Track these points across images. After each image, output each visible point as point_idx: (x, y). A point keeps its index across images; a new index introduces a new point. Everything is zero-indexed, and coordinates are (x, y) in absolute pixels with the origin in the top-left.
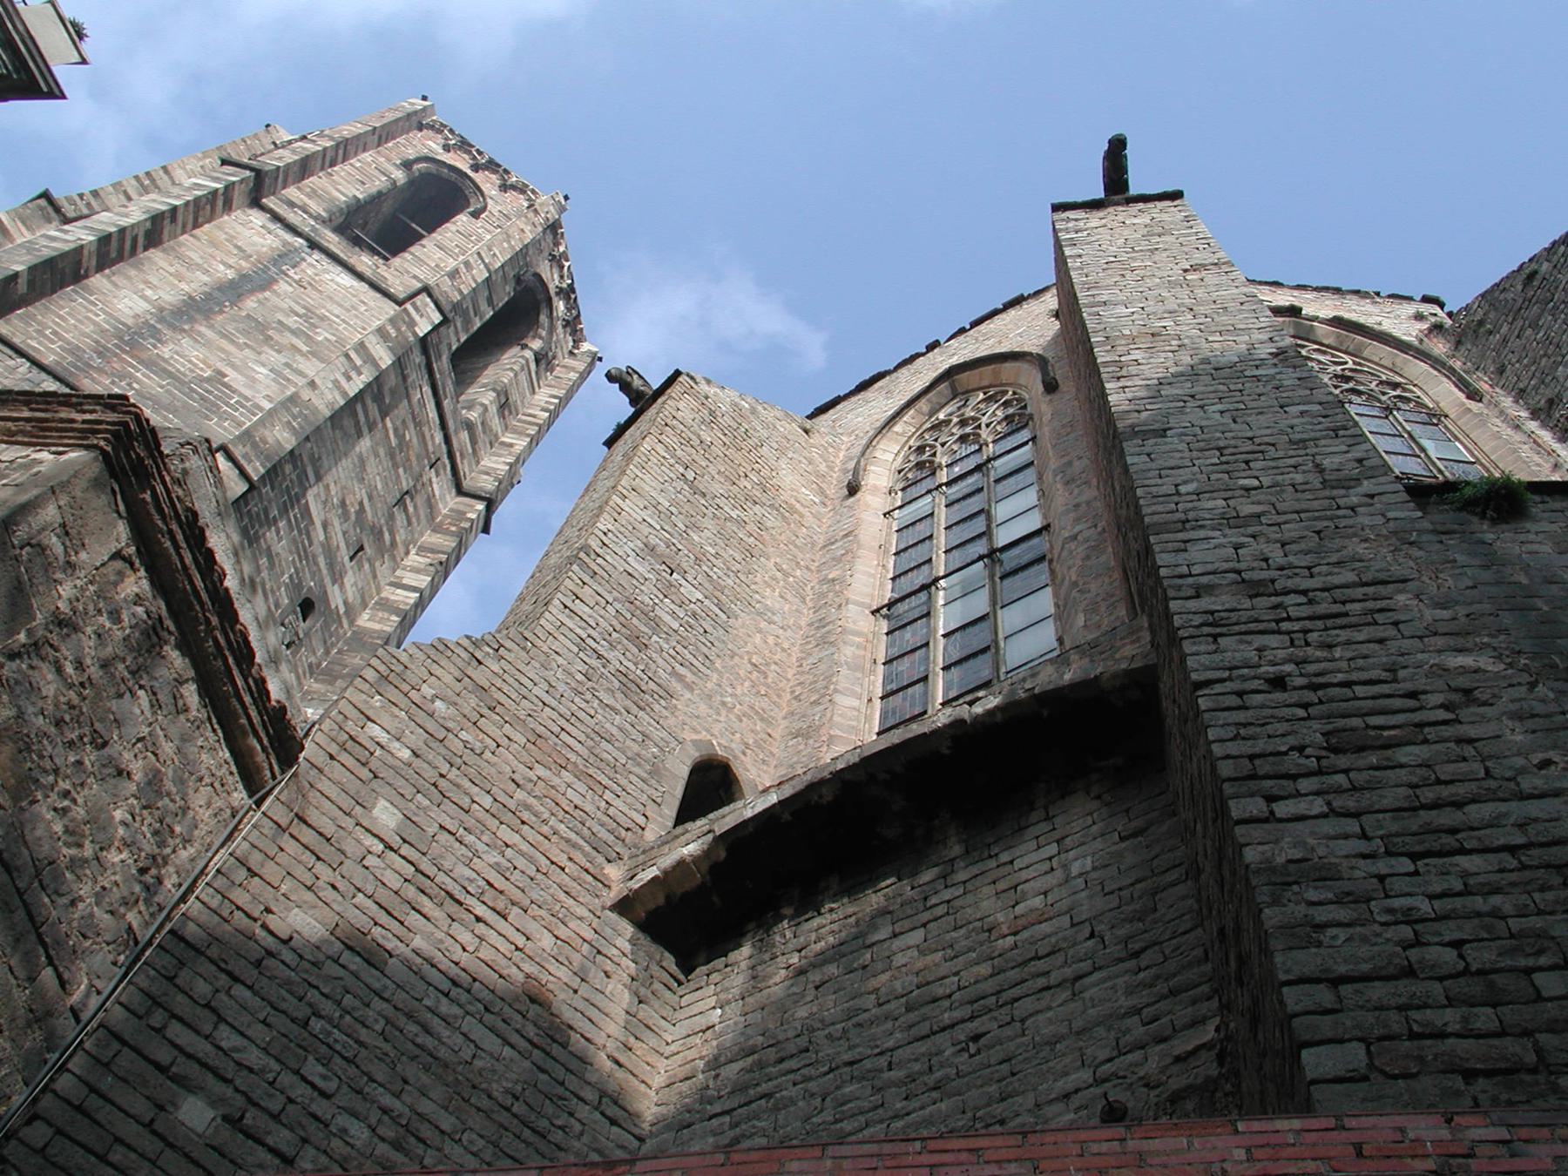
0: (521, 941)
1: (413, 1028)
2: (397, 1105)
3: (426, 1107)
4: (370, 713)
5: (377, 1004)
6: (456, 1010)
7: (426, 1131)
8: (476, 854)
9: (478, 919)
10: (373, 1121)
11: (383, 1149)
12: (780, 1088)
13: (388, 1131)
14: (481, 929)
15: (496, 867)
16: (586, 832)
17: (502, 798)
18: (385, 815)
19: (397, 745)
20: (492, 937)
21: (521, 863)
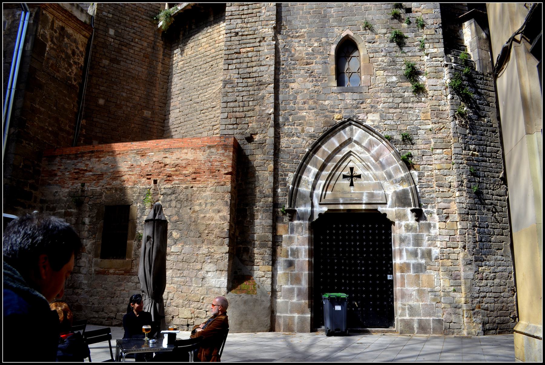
0: (141, 47)
1: (127, 73)
2: (129, 87)
3: (133, 86)
4: (102, 10)
5: (121, 71)
6: (133, 66)
7: (134, 90)
8: (129, 32)
9: (133, 46)
10: (126, 91)
11: (129, 95)
12: (187, 69)
13: (128, 92)
14: (134, 48)
15: (134, 33)
16: (148, 15)
17: (131, 16)
18: (112, 32)
19: (109, 14)
20: (136, 49)
21: (138, 29)
